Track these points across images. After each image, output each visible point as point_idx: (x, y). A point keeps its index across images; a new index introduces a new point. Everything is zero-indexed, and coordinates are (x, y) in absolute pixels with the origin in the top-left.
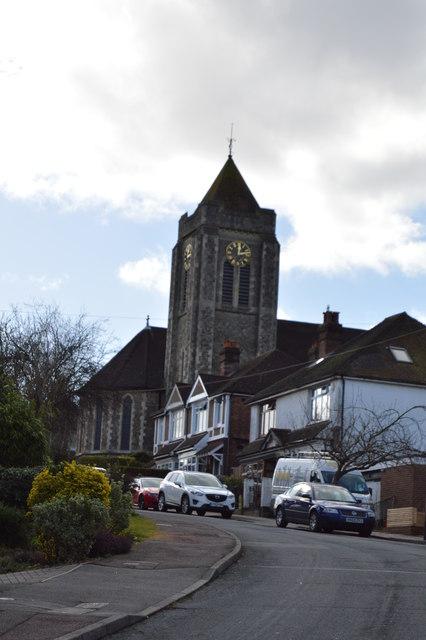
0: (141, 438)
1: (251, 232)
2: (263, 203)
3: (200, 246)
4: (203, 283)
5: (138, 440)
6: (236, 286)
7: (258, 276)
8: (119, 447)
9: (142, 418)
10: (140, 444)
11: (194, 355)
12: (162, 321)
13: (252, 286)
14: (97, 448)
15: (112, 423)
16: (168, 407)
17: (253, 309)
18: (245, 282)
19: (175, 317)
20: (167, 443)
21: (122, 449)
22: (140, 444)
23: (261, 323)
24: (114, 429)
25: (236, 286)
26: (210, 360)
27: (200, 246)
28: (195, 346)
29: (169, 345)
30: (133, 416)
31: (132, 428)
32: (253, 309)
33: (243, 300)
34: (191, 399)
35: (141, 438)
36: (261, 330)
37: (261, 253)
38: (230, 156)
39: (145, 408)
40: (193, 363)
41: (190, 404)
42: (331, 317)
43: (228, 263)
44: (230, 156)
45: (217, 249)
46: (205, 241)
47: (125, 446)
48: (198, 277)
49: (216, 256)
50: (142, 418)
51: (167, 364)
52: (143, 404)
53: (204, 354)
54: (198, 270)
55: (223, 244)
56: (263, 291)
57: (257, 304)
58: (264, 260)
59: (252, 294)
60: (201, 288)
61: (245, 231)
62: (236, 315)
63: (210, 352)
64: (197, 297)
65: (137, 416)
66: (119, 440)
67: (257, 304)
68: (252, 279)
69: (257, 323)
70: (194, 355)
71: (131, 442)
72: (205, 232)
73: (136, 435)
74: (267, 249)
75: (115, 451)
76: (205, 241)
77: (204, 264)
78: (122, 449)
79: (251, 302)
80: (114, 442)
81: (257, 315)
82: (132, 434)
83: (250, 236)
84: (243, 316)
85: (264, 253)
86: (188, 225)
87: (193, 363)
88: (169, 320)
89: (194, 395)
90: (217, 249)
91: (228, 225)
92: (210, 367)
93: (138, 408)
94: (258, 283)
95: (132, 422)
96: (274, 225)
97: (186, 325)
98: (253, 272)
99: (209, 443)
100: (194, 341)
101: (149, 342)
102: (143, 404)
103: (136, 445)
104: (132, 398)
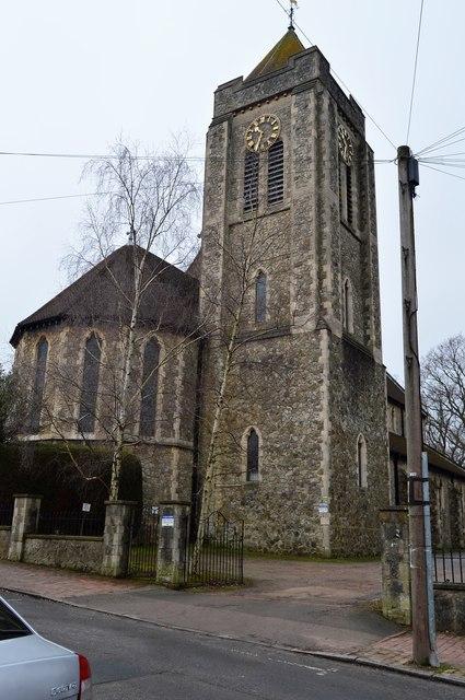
11: (321, 276)
22: (176, 426)
27: (318, 109)
37: (363, 157)
38: (291, 28)
39: (182, 363)
40: (320, 287)
44: (291, 28)
48: (319, 153)
52: (180, 358)
60: (326, 172)
68: (354, 189)
70: (321, 276)
79: (355, 220)
93: (172, 360)
94: (362, 198)
100: (320, 251)
102: (180, 358)
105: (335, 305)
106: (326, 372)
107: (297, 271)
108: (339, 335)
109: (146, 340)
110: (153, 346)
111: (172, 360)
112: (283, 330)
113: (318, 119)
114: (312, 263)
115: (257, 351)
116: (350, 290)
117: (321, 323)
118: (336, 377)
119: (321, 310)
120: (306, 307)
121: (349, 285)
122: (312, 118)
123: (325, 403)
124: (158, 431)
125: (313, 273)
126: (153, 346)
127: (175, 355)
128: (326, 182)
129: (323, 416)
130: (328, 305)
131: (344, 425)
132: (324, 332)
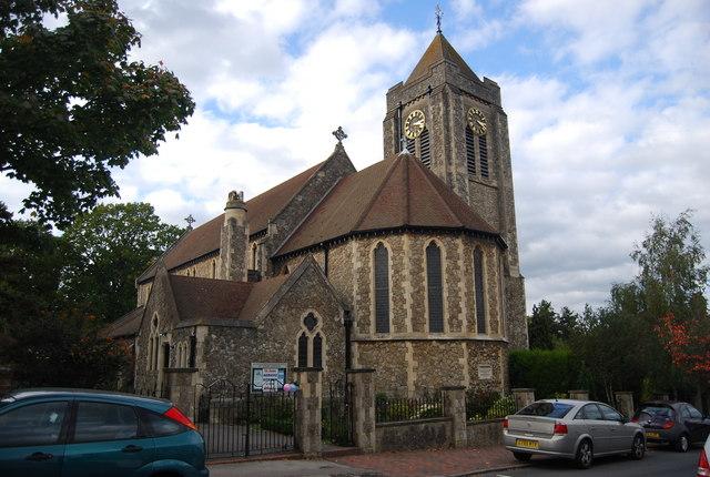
6: (477, 150)
17: (494, 184)
25: (477, 150)
33: (485, 174)
43: (469, 130)
57: (497, 176)
67: (497, 176)
86: (399, 100)
94: (497, 159)
98: (489, 140)
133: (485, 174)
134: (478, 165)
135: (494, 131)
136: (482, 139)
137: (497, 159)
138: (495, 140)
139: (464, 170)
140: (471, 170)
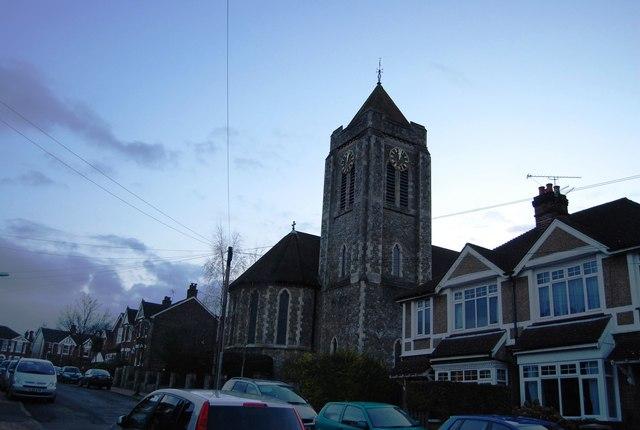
0: (298, 332)
1: (408, 142)
2: (409, 119)
3: (368, 146)
4: (372, 180)
5: (295, 335)
6: (398, 187)
7: (416, 181)
8: (275, 341)
9: (299, 312)
10: (297, 339)
12: (312, 223)
13: (410, 190)
14: (251, 341)
15: (269, 316)
16: (444, 282)
17: (412, 211)
18: (404, 185)
19: (330, 218)
20: (443, 336)
21: (278, 343)
22: (297, 339)
23: (421, 223)
24: (271, 323)
25: (398, 187)
26: (380, 254)
27: (368, 146)
28: (366, 240)
29: (324, 247)
30: (289, 311)
31: (289, 322)
32: (412, 211)
33: (404, 201)
34: (526, 262)
35: (298, 332)
36: (421, 230)
38: (379, 83)
39: (302, 303)
40: (364, 255)
41: (524, 269)
42: (549, 202)
43: (390, 166)
45: (383, 150)
46: (373, 141)
47: (281, 340)
49: (383, 156)
50: (299, 312)
51: (323, 263)
52: (300, 299)
53: (375, 251)
54: (367, 168)
55: (388, 148)
56: (421, 195)
57: (416, 206)
58: (421, 167)
59: (410, 197)
60: (370, 186)
61: (404, 141)
62: (398, 214)
63: (380, 247)
64: (366, 192)
65: (295, 310)
66: (275, 335)
68: (411, 184)
69: (416, 224)
70: (365, 248)
71: (287, 336)
72: (374, 133)
73: (293, 330)
74: (423, 157)
75: (270, 345)
76: (373, 141)
77: (373, 163)
78: (278, 343)
79: (410, 204)
80: (270, 336)
81: (416, 216)
82: (288, 328)
83: (407, 146)
84: (404, 217)
85: (421, 161)
87: (364, 255)
88: (323, 221)
89: (537, 255)
90: (383, 150)
91: (390, 132)
92: (380, 261)
93: (295, 302)
94: (417, 187)
95: (289, 317)
96: (425, 139)
97: (349, 222)
98: (410, 176)
99: (616, 337)
101: (295, 246)
102: (300, 299)
103: (293, 340)
104: (289, 292)
105: (374, 265)
106: (363, 305)
107: (354, 247)
108: (377, 281)
109: (281, 292)
110: (285, 296)
111: (295, 302)
112: (346, 282)
113: (367, 153)
114: (361, 244)
115: (338, 293)
116: (401, 250)
117: (364, 278)
118: (372, 307)
119: (365, 269)
120: (356, 268)
121: (400, 247)
122: (363, 153)
123: (361, 322)
124: (287, 343)
125: (360, 248)
126: (285, 296)
127: (299, 297)
128: (371, 192)
129: (360, 331)
130: (368, 265)
131: (380, 335)
132: (362, 283)
133: (404, 201)
134: (398, 196)
135: (417, 168)
136: (404, 175)
137: (417, 187)
138: (416, 174)
139: (381, 201)
140: (390, 198)
